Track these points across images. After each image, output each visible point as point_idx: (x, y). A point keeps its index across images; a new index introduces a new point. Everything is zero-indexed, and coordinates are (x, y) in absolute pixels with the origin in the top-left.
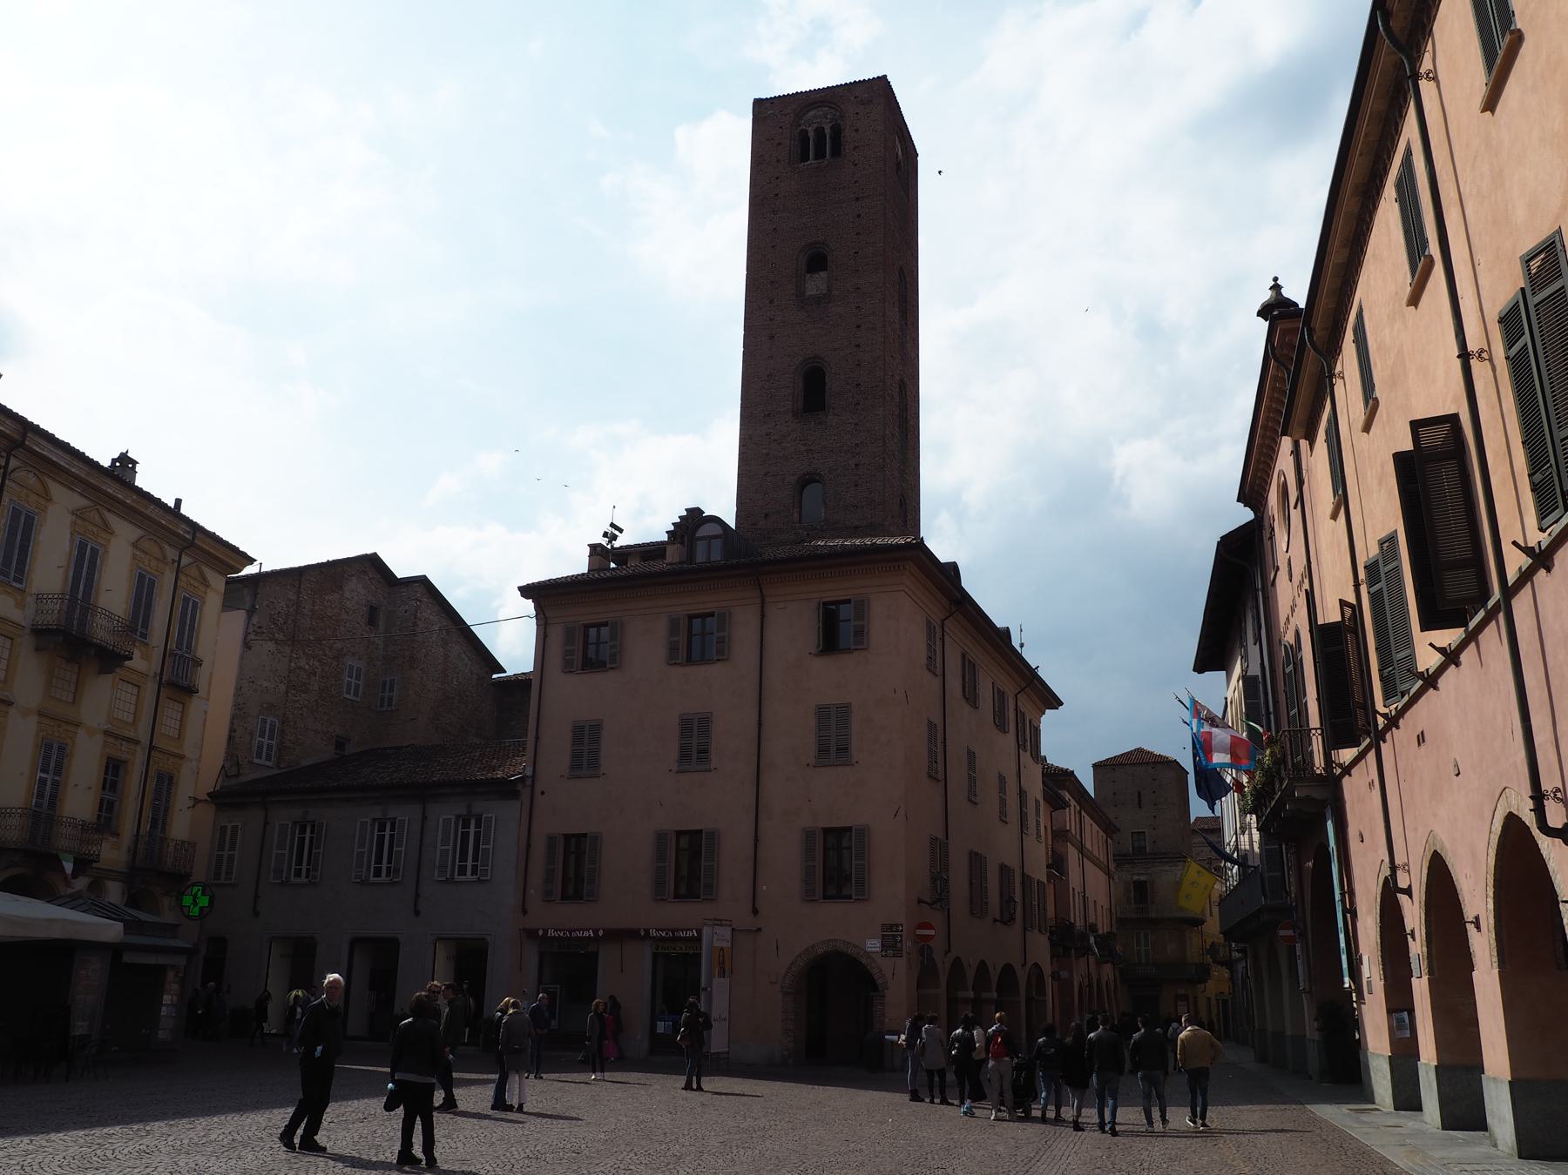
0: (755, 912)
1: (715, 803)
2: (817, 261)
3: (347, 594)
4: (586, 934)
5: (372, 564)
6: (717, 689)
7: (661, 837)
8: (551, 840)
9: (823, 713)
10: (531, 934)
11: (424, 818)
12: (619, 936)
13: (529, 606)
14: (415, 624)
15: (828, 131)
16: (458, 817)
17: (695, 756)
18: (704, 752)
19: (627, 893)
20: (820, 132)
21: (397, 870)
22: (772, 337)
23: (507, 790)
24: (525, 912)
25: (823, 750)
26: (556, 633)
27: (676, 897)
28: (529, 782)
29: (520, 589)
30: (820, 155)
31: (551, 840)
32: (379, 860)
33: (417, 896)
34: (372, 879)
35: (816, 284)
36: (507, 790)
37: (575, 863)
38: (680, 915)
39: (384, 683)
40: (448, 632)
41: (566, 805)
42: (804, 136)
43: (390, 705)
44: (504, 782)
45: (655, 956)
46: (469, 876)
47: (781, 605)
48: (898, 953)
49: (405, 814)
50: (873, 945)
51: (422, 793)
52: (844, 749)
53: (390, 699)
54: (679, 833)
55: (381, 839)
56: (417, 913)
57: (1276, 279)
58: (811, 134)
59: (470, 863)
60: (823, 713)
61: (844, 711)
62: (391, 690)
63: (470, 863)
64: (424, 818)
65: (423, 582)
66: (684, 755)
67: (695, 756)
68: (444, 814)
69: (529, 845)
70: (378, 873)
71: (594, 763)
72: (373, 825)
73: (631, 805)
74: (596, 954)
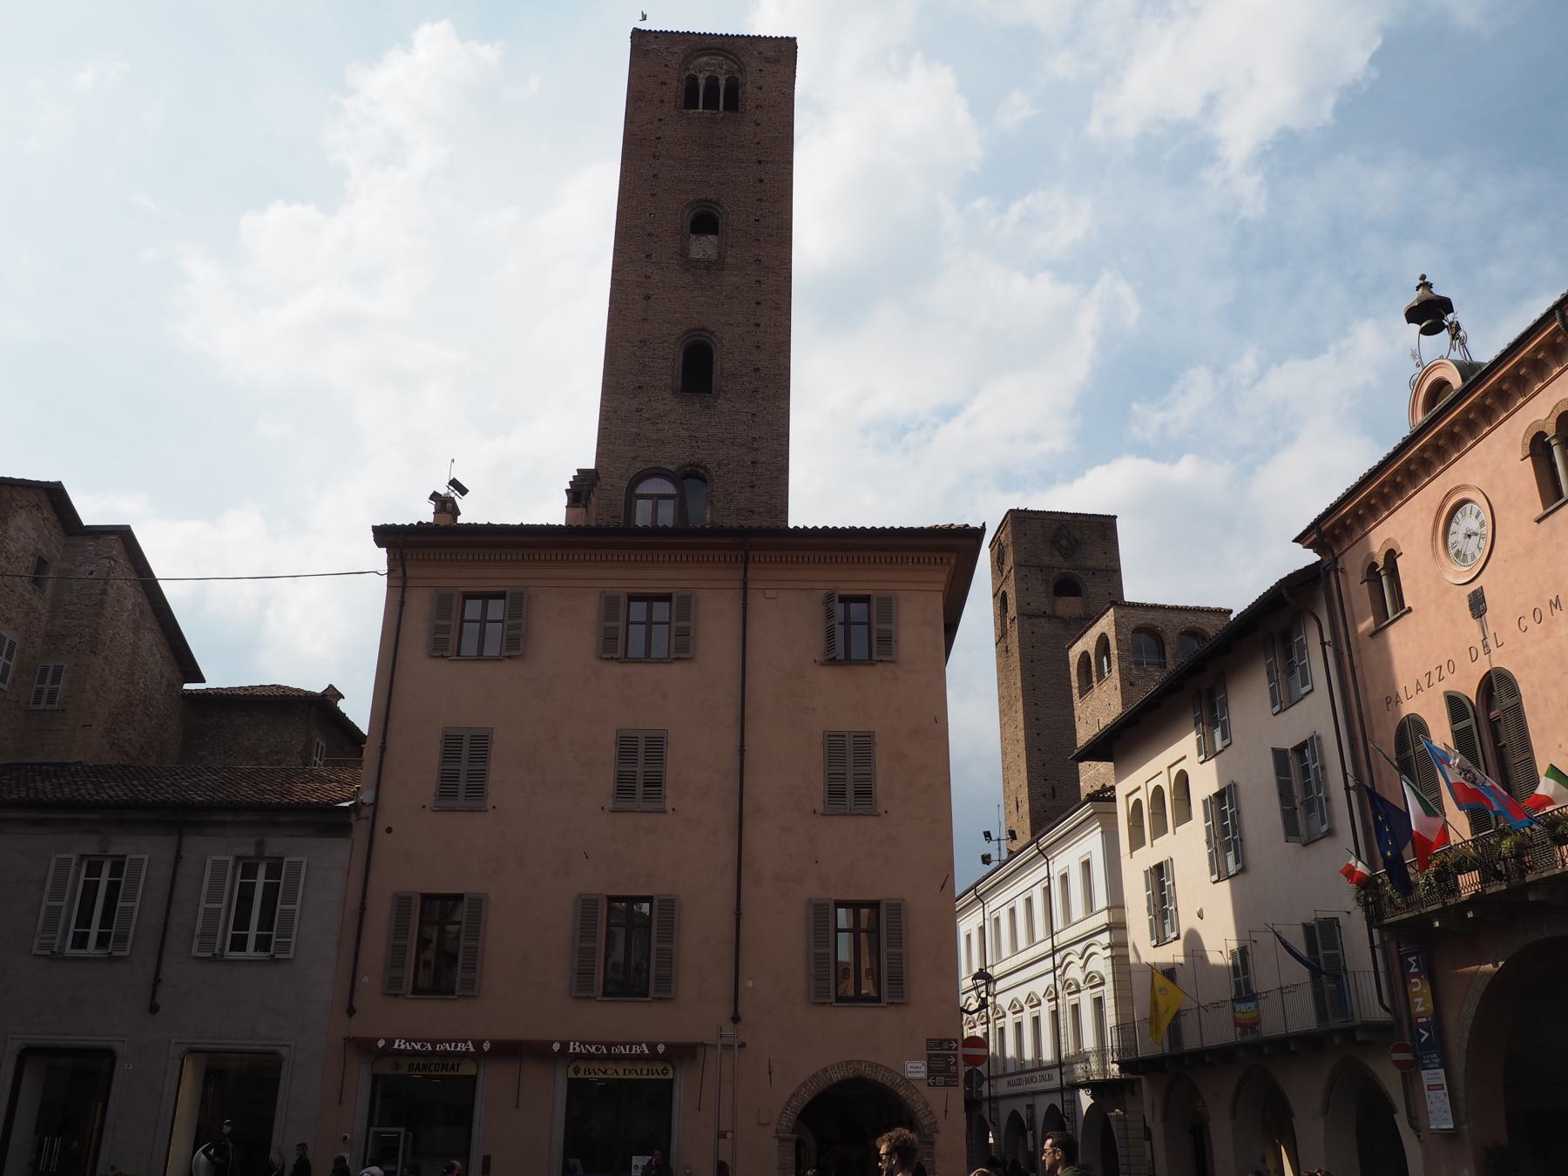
0: (736, 1019)
1: (670, 856)
2: (705, 223)
3: (12, 532)
4: (461, 1047)
5: (53, 496)
6: (678, 702)
7: (587, 904)
8: (402, 902)
9: (834, 743)
10: (363, 1047)
11: (178, 858)
12: (508, 1051)
13: (379, 558)
14: (104, 592)
15: (722, 83)
16: (238, 858)
17: (640, 789)
18: (654, 785)
19: (527, 983)
20: (712, 84)
21: (121, 939)
22: (647, 298)
23: (330, 821)
24: (351, 1011)
25: (835, 793)
26: (421, 602)
27: (605, 994)
28: (366, 812)
29: (375, 529)
30: (711, 103)
31: (402, 902)
32: (85, 919)
33: (157, 981)
34: (68, 951)
35: (704, 247)
36: (330, 821)
37: (440, 944)
38: (633, 1025)
39: (45, 671)
40: (142, 612)
41: (424, 848)
42: (692, 83)
43: (51, 700)
44: (329, 809)
45: (375, 1078)
46: (250, 951)
47: (769, 593)
48: (951, 1082)
49: (145, 852)
50: (916, 1069)
51: (179, 819)
52: (865, 793)
53: (53, 693)
54: (612, 899)
55: (90, 890)
56: (154, 1009)
57: (1423, 277)
58: (702, 82)
59: (253, 933)
60: (834, 743)
61: (864, 743)
62: (56, 679)
63: (253, 933)
64: (178, 858)
65: (123, 537)
66: (624, 788)
67: (640, 789)
68: (214, 856)
69: (363, 908)
70: (80, 941)
71: (477, 789)
72: (79, 865)
73: (537, 857)
74: (474, 1078)
